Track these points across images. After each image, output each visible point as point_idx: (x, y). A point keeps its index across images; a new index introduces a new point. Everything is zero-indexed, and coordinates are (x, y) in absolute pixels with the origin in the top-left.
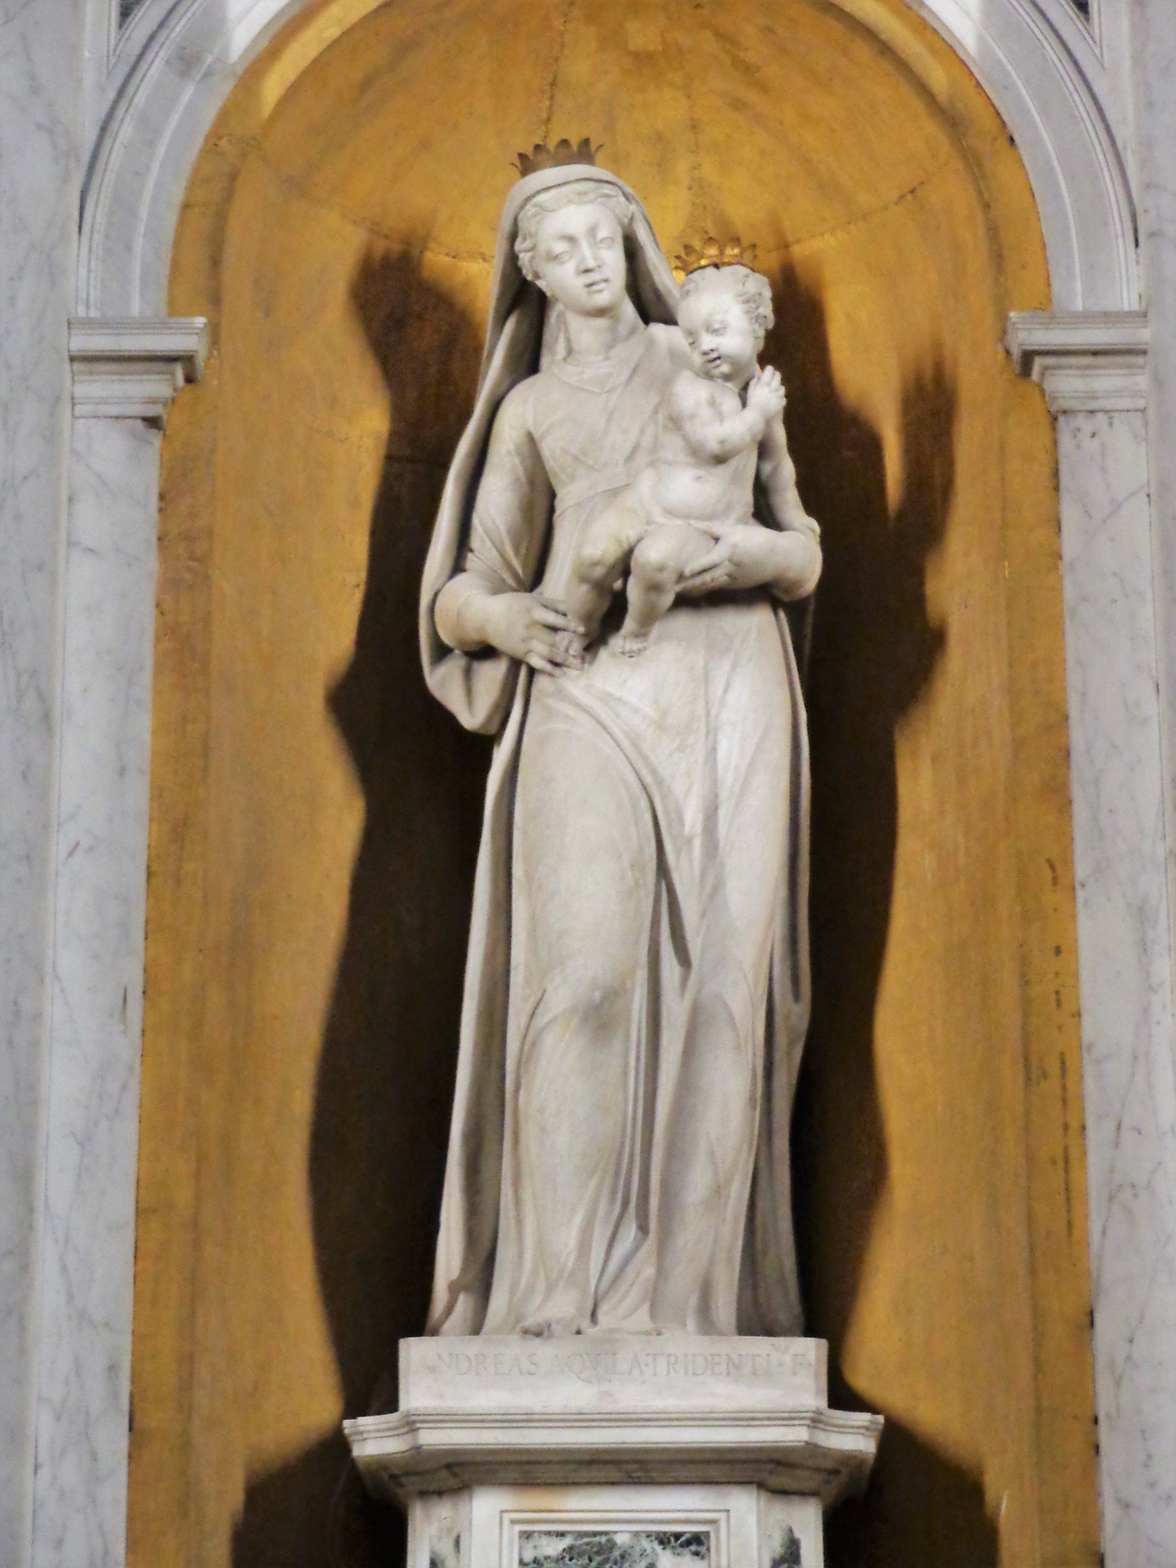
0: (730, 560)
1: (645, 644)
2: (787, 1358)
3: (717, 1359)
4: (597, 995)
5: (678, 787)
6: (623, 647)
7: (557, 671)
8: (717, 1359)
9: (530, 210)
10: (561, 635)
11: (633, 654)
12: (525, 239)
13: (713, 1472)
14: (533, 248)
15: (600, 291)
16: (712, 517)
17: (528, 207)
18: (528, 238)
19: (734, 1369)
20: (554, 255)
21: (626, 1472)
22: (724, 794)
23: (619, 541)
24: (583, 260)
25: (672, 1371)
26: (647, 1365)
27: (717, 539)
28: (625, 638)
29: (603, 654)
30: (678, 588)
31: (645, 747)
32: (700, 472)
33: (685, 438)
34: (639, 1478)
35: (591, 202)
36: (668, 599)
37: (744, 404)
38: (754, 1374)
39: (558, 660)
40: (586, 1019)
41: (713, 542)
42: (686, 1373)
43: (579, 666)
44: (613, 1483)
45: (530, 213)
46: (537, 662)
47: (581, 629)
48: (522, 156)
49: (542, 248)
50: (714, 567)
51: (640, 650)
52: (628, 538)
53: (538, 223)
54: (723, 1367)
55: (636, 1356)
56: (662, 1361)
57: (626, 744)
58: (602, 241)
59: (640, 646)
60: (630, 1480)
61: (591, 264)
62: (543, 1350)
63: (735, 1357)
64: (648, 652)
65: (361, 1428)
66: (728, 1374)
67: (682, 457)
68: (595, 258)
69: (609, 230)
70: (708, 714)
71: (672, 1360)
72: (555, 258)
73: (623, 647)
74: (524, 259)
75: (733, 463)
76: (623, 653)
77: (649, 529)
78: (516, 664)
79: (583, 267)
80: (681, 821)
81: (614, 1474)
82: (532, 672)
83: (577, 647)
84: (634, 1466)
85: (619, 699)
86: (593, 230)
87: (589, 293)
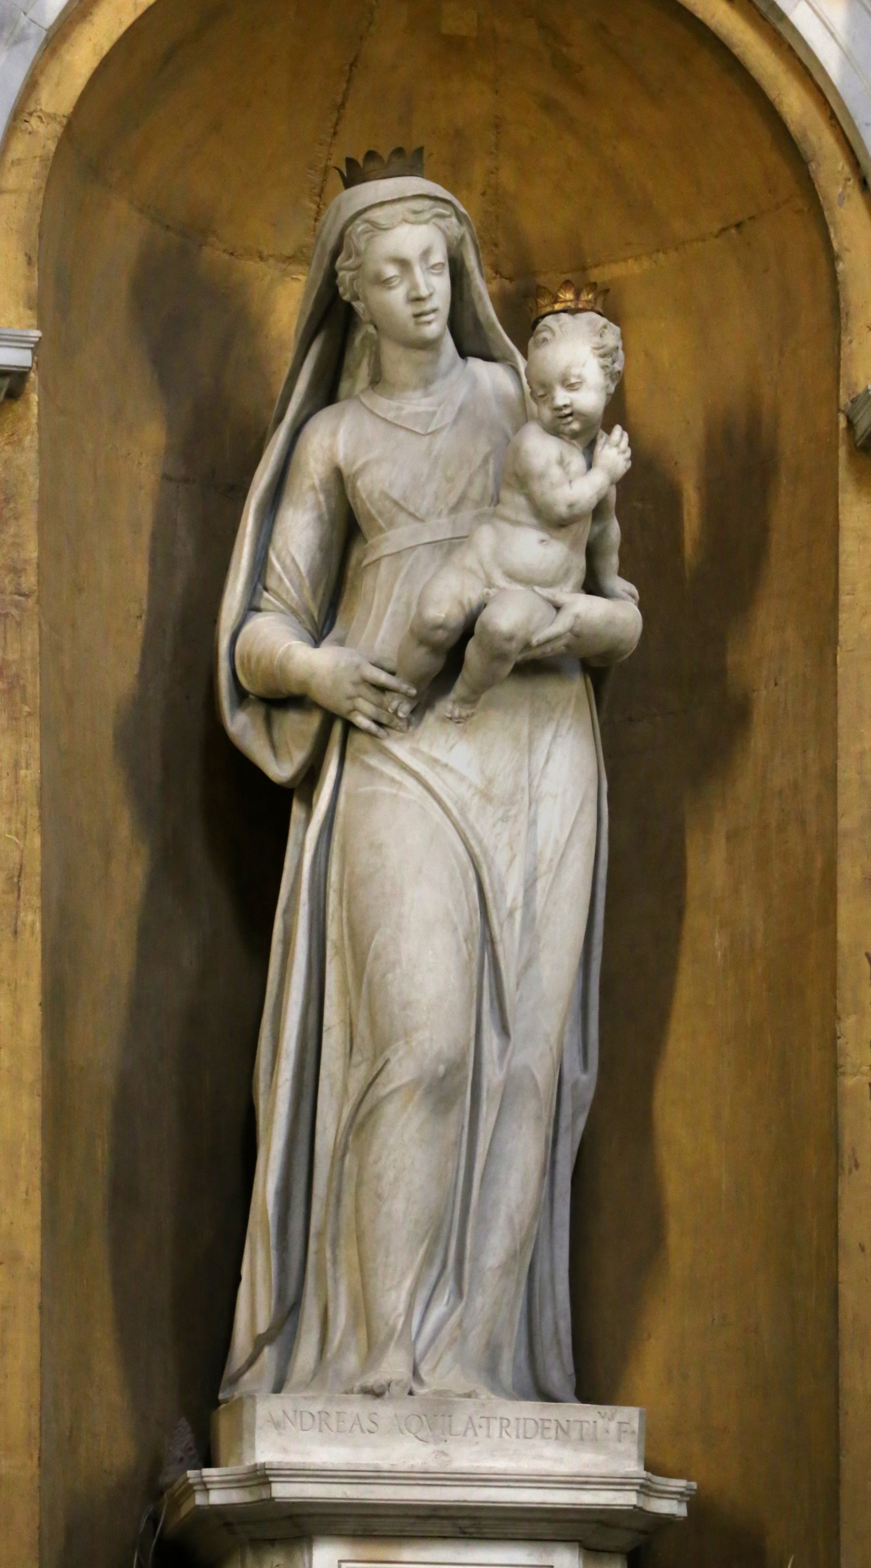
0: (571, 630)
1: (473, 711)
2: (613, 1426)
3: (547, 1424)
4: (442, 1069)
5: (501, 858)
6: (452, 712)
7: (381, 732)
8: (547, 1424)
9: (360, 227)
10: (388, 697)
11: (461, 720)
12: (349, 257)
13: (541, 1529)
14: (358, 267)
15: (429, 323)
16: (551, 584)
17: (358, 222)
18: (354, 256)
19: (563, 1434)
20: (384, 278)
21: (460, 1528)
22: (543, 868)
23: (461, 603)
24: (415, 286)
25: (504, 1434)
26: (480, 1427)
27: (558, 608)
28: (454, 702)
29: (430, 718)
30: (520, 658)
31: (471, 816)
32: (542, 535)
33: (530, 498)
34: (471, 1533)
35: (426, 222)
36: (509, 667)
37: (590, 466)
38: (582, 1439)
39: (384, 720)
40: (428, 1092)
41: (554, 611)
42: (518, 1437)
43: (405, 728)
44: (445, 1538)
45: (360, 229)
46: (362, 721)
47: (413, 692)
48: (350, 162)
49: (371, 268)
50: (558, 637)
51: (468, 716)
52: (469, 599)
53: (368, 240)
54: (552, 1433)
55: (470, 1418)
56: (495, 1425)
57: (455, 812)
58: (433, 267)
59: (469, 712)
60: (462, 1535)
61: (424, 292)
62: (384, 1410)
63: (564, 1425)
64: (475, 718)
65: (206, 1479)
66: (557, 1438)
67: (526, 517)
68: (428, 285)
69: (439, 256)
70: (530, 785)
71: (505, 1422)
72: (385, 283)
73: (452, 712)
74: (345, 276)
75: (575, 527)
76: (451, 719)
77: (492, 592)
78: (329, 718)
79: (414, 294)
80: (503, 892)
81: (449, 1530)
82: (349, 727)
83: (405, 710)
84: (466, 1522)
85: (446, 766)
86: (426, 254)
87: (418, 324)
